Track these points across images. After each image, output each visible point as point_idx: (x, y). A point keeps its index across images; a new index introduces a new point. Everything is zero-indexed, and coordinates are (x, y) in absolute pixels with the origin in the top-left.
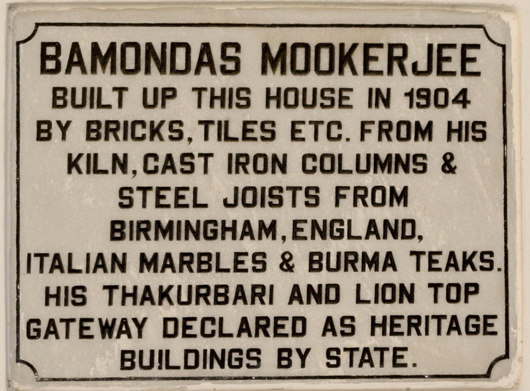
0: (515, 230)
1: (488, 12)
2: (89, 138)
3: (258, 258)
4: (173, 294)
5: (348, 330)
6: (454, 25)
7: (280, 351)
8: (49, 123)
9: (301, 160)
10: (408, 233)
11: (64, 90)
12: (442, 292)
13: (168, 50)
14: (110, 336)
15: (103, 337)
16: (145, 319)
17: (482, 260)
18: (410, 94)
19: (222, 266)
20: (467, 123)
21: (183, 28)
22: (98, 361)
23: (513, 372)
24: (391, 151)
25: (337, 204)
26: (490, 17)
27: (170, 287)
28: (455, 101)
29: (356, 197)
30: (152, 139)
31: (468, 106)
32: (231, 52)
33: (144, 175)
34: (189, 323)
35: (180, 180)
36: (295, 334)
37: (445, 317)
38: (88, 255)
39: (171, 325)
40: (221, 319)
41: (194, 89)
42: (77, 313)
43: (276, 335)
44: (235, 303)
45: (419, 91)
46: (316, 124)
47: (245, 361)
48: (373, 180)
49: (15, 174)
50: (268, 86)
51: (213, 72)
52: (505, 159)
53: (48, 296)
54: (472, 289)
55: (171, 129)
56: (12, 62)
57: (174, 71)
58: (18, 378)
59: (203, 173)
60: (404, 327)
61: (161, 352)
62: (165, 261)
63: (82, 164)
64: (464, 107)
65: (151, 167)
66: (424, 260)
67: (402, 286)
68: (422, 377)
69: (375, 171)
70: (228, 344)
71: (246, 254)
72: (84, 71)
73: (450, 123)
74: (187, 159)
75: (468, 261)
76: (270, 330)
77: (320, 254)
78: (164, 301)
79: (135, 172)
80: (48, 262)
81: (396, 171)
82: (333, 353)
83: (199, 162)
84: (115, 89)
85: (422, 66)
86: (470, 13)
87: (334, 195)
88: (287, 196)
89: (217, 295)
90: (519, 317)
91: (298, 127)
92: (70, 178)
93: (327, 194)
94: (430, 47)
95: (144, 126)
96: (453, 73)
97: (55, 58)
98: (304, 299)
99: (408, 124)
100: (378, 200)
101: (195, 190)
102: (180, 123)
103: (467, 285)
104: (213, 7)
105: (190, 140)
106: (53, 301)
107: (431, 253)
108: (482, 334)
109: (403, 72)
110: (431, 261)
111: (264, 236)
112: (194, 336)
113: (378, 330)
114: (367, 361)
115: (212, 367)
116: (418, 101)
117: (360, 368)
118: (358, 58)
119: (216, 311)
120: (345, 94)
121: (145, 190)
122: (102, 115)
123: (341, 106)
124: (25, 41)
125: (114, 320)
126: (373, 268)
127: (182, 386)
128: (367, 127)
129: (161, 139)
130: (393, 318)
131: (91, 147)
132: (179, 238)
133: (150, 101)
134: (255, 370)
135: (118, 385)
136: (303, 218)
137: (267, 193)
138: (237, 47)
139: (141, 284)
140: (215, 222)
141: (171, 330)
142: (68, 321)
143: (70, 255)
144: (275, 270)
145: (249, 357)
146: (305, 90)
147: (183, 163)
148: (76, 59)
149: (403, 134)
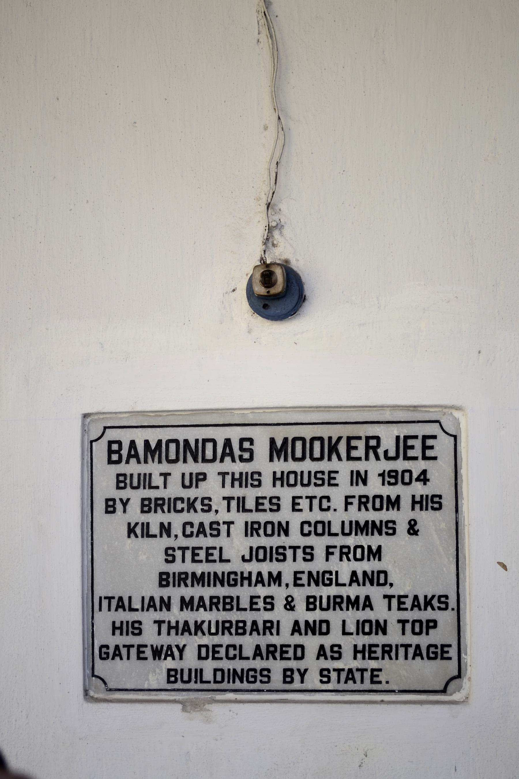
0: (465, 578)
1: (442, 410)
2: (143, 511)
3: (268, 600)
4: (205, 626)
5: (336, 655)
7: (285, 670)
8: (114, 500)
10: (382, 581)
11: (125, 475)
12: (408, 626)
14: (160, 659)
15: (154, 659)
16: (184, 646)
17: (440, 602)
18: (382, 475)
19: (241, 606)
20: (427, 496)
21: (210, 428)
22: (150, 676)
23: (464, 689)
24: (368, 518)
25: (327, 560)
27: (203, 622)
28: (418, 479)
29: (342, 553)
30: (188, 511)
31: (428, 483)
32: (246, 445)
33: (183, 538)
34: (217, 649)
35: (210, 542)
36: (296, 658)
37: (410, 646)
38: (143, 598)
39: (204, 651)
40: (241, 646)
41: (219, 474)
42: (136, 640)
43: (282, 658)
44: (251, 634)
45: (390, 472)
46: (311, 498)
47: (259, 678)
48: (354, 541)
49: (90, 538)
50: (274, 470)
51: (233, 460)
52: (457, 523)
53: (114, 628)
54: (431, 624)
55: (203, 504)
56: (87, 455)
57: (204, 460)
58: (93, 688)
60: (379, 654)
61: (196, 670)
62: (199, 603)
63: (138, 530)
64: (425, 484)
65: (188, 532)
66: (394, 602)
67: (377, 622)
68: (393, 691)
69: (356, 534)
70: (246, 665)
71: (259, 597)
72: (139, 462)
73: (413, 497)
74: (215, 526)
75: (428, 603)
76: (278, 655)
77: (314, 597)
78: (198, 632)
80: (114, 603)
81: (373, 534)
82: (325, 673)
83: (223, 528)
84: (161, 474)
85: (392, 453)
86: (429, 412)
87: (325, 552)
88: (289, 553)
89: (237, 628)
90: (469, 646)
91: (297, 501)
92: (129, 541)
93: (319, 552)
94: (398, 438)
95: (183, 502)
96: (415, 458)
97: (118, 452)
98: (303, 631)
99: (381, 497)
100: (359, 556)
101: (221, 549)
102: (210, 499)
103: (428, 621)
104: (233, 411)
105: (217, 511)
106: (118, 632)
107: (400, 597)
108: (440, 659)
109: (377, 458)
110: (400, 603)
111: (272, 583)
112: (221, 659)
113: (359, 656)
114: (350, 679)
115: (234, 682)
116: (389, 480)
117: (346, 685)
118: (342, 448)
119: (237, 640)
120: (333, 475)
121: (184, 549)
122: (153, 494)
123: (330, 485)
124: (96, 440)
125: (162, 646)
126: (355, 608)
127: (212, 696)
128: (350, 500)
129: (196, 511)
130: (371, 646)
131: (144, 518)
132: (209, 585)
133: (187, 483)
134: (266, 684)
135: (165, 695)
136: (301, 570)
137: (274, 551)
138: (251, 441)
139: (182, 619)
140: (235, 573)
141: (203, 654)
142: (129, 647)
144: (281, 609)
145: (262, 675)
146: (302, 472)
147: (211, 528)
149: (378, 505)
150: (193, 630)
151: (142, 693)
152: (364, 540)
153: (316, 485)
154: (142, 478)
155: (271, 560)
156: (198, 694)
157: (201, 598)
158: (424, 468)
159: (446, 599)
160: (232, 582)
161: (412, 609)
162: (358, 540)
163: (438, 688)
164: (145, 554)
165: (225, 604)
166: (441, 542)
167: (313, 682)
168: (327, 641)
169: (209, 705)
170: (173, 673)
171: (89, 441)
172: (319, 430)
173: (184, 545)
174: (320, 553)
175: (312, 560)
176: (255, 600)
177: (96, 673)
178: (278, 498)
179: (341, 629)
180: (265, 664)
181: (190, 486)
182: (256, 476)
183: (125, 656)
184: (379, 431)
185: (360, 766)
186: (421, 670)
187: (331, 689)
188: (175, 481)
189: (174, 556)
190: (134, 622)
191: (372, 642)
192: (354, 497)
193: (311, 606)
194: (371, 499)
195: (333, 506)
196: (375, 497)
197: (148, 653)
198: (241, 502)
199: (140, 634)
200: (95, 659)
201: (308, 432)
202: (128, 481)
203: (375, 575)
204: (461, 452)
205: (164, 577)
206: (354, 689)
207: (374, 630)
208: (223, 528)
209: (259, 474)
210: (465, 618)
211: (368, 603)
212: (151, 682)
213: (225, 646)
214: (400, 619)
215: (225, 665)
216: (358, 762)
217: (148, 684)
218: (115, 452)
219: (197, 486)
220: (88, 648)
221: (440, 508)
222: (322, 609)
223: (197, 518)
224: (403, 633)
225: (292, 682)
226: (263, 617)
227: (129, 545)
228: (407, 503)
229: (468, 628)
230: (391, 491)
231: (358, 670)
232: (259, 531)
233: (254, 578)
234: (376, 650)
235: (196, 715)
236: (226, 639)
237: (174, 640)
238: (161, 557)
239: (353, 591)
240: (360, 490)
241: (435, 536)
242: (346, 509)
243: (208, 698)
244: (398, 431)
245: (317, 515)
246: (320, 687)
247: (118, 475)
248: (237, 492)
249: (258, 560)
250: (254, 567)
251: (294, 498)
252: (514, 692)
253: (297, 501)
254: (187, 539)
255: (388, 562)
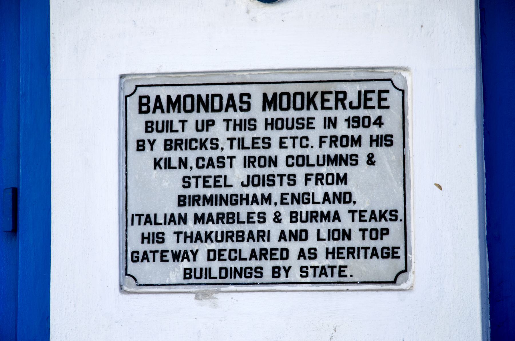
0: (410, 197)
1: (393, 71)
2: (166, 149)
3: (261, 215)
4: (213, 236)
5: (313, 256)
6: (373, 79)
7: (274, 268)
8: (143, 141)
9: (285, 159)
10: (347, 199)
11: (152, 122)
12: (367, 234)
13: (210, 99)
14: (178, 261)
15: (174, 261)
16: (197, 251)
17: (391, 215)
18: (348, 120)
19: (241, 220)
20: (382, 136)
21: (218, 86)
22: (171, 274)
25: (306, 184)
26: (395, 74)
27: (211, 232)
28: (375, 123)
30: (201, 149)
31: (382, 126)
32: (245, 98)
33: (197, 169)
34: (222, 253)
35: (216, 172)
36: (282, 258)
37: (369, 248)
38: (166, 215)
39: (212, 254)
40: (240, 250)
41: (224, 120)
42: (159, 247)
43: (272, 259)
44: (248, 241)
45: (354, 118)
46: (294, 138)
47: (254, 274)
48: (326, 170)
49: (125, 170)
50: (266, 118)
51: (235, 110)
52: (404, 156)
53: (143, 238)
54: (385, 232)
55: (212, 143)
57: (213, 110)
58: (126, 284)
59: (230, 167)
60: (345, 254)
61: (206, 269)
62: (208, 218)
63: (162, 164)
64: (380, 127)
65: (200, 164)
66: (357, 215)
67: (344, 230)
68: (356, 283)
69: (328, 165)
70: (244, 264)
71: (254, 213)
72: (163, 112)
73: (371, 136)
74: (221, 160)
75: (382, 216)
76: (268, 256)
77: (296, 213)
78: (208, 240)
79: (191, 168)
80: (143, 219)
81: (340, 165)
82: (304, 269)
83: (227, 161)
84: (180, 121)
85: (355, 104)
87: (304, 179)
88: (277, 180)
89: (238, 236)
90: (413, 247)
91: (284, 140)
92: (155, 172)
94: (360, 92)
95: (196, 142)
96: (373, 108)
97: (147, 104)
98: (288, 238)
99: (347, 137)
100: (330, 181)
101: (225, 177)
102: (217, 140)
103: (382, 230)
104: (235, 73)
105: (222, 149)
106: (146, 241)
107: (361, 211)
108: (391, 258)
109: (344, 108)
110: (361, 216)
111: (264, 202)
112: (225, 260)
113: (330, 256)
114: (323, 274)
115: (235, 277)
116: (353, 124)
117: (320, 278)
118: (318, 100)
119: (237, 246)
120: (310, 121)
121: (197, 178)
122: (173, 136)
123: (308, 128)
125: (180, 251)
126: (327, 221)
127: (219, 288)
128: (323, 139)
129: (206, 149)
130: (339, 249)
131: (166, 154)
132: (216, 205)
133: (200, 127)
134: (260, 279)
136: (286, 192)
137: (266, 178)
138: (249, 95)
139: (195, 230)
140: (236, 195)
141: (212, 256)
142: (154, 252)
143: (155, 215)
144: (271, 222)
145: (256, 272)
146: (287, 119)
147: (218, 162)
148: (158, 105)
149: (344, 143)
150: (203, 238)
151: (164, 287)
152: (334, 169)
153: (298, 128)
154: (165, 124)
155: (264, 185)
156: (207, 287)
157: (210, 215)
158: (380, 115)
159: (396, 213)
160: (234, 202)
161: (370, 221)
162: (330, 169)
163: (390, 280)
164: (167, 182)
165: (228, 218)
166: (392, 170)
167: (295, 276)
168: (306, 245)
169: (216, 294)
170: (188, 271)
171: (124, 96)
172: (300, 87)
173: (197, 175)
174: (300, 179)
175: (294, 184)
176: (251, 215)
177: (129, 273)
178: (269, 139)
179: (316, 236)
180: (259, 263)
181: (202, 130)
182: (252, 122)
183: (151, 259)
184: (345, 88)
185: (331, 339)
186: (377, 267)
187: (308, 281)
188: (190, 126)
189: (189, 183)
190: (158, 233)
191: (339, 246)
192: (326, 137)
193: (294, 219)
194: (339, 139)
195: (310, 144)
196: (342, 137)
197: (169, 256)
198: (241, 142)
199: (163, 242)
200: (128, 262)
201: (292, 89)
202: (154, 127)
203: (342, 195)
204: (407, 103)
205: (182, 198)
206: (326, 281)
207: (341, 237)
208: (227, 161)
209: (255, 120)
210: (411, 227)
211: (337, 217)
212: (171, 279)
213: (228, 251)
214: (361, 228)
215: (228, 265)
216: (329, 336)
217: (169, 280)
218: (145, 104)
219: (207, 130)
220: (123, 253)
221: (391, 145)
222: (302, 221)
223: (207, 154)
224: (364, 239)
225: (279, 276)
226: (257, 228)
227: (155, 175)
228: (367, 141)
229: (412, 234)
230: (354, 133)
231: (329, 267)
232: (254, 163)
233: (250, 199)
234: (343, 252)
235: (206, 302)
236: (229, 245)
237: (189, 246)
238: (179, 184)
239: (325, 208)
240: (331, 132)
241: (388, 166)
242: (320, 146)
243: (215, 290)
244: (360, 87)
245: (298, 151)
246: (301, 280)
247: (147, 122)
248: (238, 134)
249: (254, 185)
250: (250, 190)
251: (281, 138)
252: (447, 281)
253: (284, 140)
254: (200, 169)
255: (352, 186)
